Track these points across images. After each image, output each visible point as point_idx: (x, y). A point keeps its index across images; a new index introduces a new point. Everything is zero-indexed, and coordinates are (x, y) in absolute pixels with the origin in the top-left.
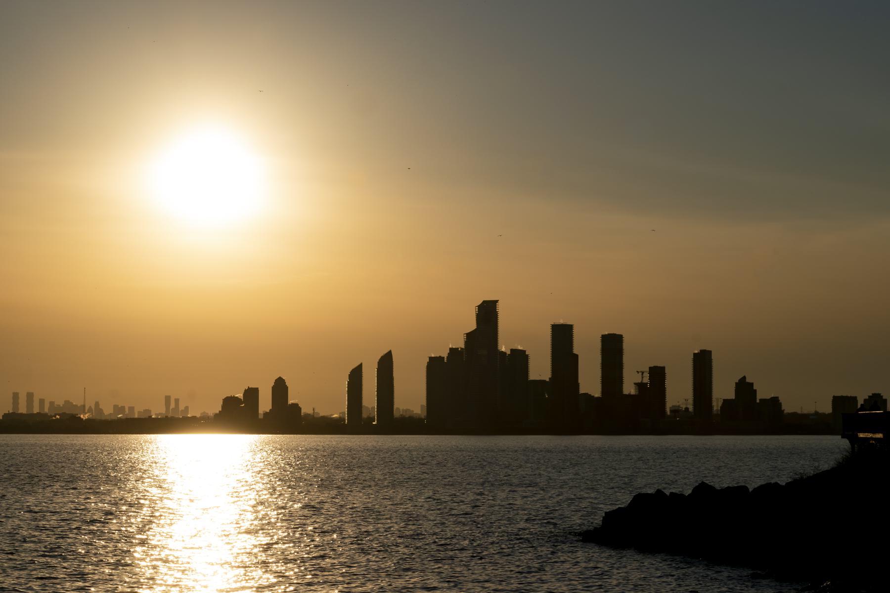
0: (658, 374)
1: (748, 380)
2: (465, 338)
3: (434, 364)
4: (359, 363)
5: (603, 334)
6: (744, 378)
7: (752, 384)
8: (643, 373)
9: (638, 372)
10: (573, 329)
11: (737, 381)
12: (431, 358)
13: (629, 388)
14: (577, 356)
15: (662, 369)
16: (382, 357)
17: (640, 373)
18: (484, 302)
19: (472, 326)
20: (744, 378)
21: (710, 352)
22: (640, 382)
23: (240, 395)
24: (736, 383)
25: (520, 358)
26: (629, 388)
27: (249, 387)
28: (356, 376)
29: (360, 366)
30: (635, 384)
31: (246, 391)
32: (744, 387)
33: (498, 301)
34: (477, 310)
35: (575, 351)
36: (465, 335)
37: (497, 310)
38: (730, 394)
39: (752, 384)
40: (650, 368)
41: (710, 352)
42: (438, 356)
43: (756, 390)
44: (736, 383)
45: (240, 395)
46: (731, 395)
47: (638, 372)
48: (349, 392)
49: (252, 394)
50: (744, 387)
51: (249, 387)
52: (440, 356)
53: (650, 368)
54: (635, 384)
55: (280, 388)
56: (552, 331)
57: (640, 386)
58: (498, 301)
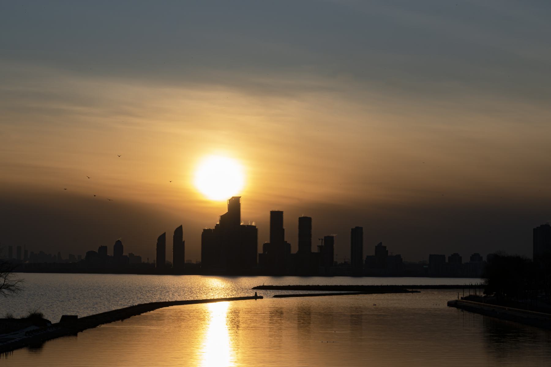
0: (329, 241)
1: (383, 245)
2: (220, 218)
3: (207, 234)
4: (164, 232)
5: (300, 216)
6: (381, 243)
7: (385, 247)
8: (322, 240)
9: (319, 239)
10: (283, 214)
11: (376, 245)
12: (204, 230)
13: (314, 249)
14: (284, 229)
15: (333, 237)
16: (176, 229)
17: (321, 240)
18: (233, 197)
19: (227, 211)
20: (381, 243)
21: (362, 228)
22: (321, 245)
23: (97, 252)
24: (376, 247)
25: (251, 230)
26: (314, 249)
27: (101, 246)
28: (162, 239)
29: (164, 234)
30: (318, 246)
31: (100, 248)
32: (381, 249)
33: (241, 197)
34: (228, 202)
35: (284, 227)
36: (220, 217)
37: (240, 202)
38: (373, 253)
39: (385, 247)
40: (325, 237)
41: (362, 228)
42: (209, 229)
43: (387, 251)
44: (376, 247)
45: (97, 252)
46: (373, 253)
47: (319, 239)
48: (157, 249)
49: (103, 249)
50: (381, 249)
51: (101, 246)
52: (210, 229)
53: (325, 237)
54: (318, 246)
55: (119, 246)
56: (271, 215)
57: (320, 247)
58: (241, 197)
